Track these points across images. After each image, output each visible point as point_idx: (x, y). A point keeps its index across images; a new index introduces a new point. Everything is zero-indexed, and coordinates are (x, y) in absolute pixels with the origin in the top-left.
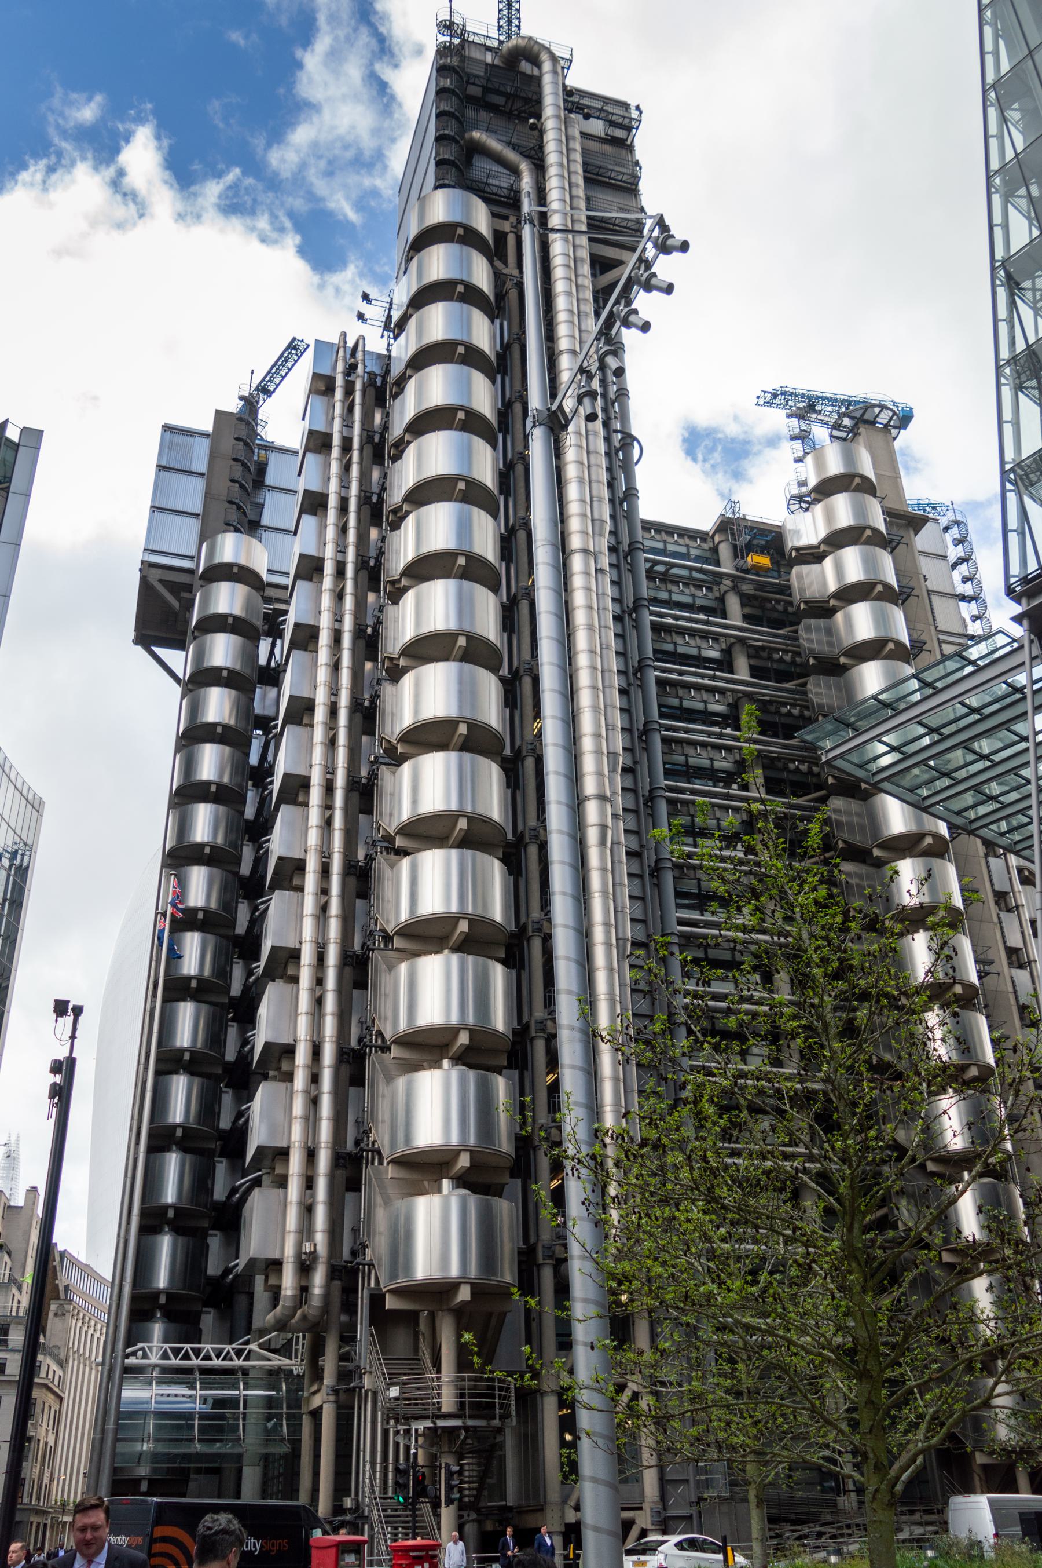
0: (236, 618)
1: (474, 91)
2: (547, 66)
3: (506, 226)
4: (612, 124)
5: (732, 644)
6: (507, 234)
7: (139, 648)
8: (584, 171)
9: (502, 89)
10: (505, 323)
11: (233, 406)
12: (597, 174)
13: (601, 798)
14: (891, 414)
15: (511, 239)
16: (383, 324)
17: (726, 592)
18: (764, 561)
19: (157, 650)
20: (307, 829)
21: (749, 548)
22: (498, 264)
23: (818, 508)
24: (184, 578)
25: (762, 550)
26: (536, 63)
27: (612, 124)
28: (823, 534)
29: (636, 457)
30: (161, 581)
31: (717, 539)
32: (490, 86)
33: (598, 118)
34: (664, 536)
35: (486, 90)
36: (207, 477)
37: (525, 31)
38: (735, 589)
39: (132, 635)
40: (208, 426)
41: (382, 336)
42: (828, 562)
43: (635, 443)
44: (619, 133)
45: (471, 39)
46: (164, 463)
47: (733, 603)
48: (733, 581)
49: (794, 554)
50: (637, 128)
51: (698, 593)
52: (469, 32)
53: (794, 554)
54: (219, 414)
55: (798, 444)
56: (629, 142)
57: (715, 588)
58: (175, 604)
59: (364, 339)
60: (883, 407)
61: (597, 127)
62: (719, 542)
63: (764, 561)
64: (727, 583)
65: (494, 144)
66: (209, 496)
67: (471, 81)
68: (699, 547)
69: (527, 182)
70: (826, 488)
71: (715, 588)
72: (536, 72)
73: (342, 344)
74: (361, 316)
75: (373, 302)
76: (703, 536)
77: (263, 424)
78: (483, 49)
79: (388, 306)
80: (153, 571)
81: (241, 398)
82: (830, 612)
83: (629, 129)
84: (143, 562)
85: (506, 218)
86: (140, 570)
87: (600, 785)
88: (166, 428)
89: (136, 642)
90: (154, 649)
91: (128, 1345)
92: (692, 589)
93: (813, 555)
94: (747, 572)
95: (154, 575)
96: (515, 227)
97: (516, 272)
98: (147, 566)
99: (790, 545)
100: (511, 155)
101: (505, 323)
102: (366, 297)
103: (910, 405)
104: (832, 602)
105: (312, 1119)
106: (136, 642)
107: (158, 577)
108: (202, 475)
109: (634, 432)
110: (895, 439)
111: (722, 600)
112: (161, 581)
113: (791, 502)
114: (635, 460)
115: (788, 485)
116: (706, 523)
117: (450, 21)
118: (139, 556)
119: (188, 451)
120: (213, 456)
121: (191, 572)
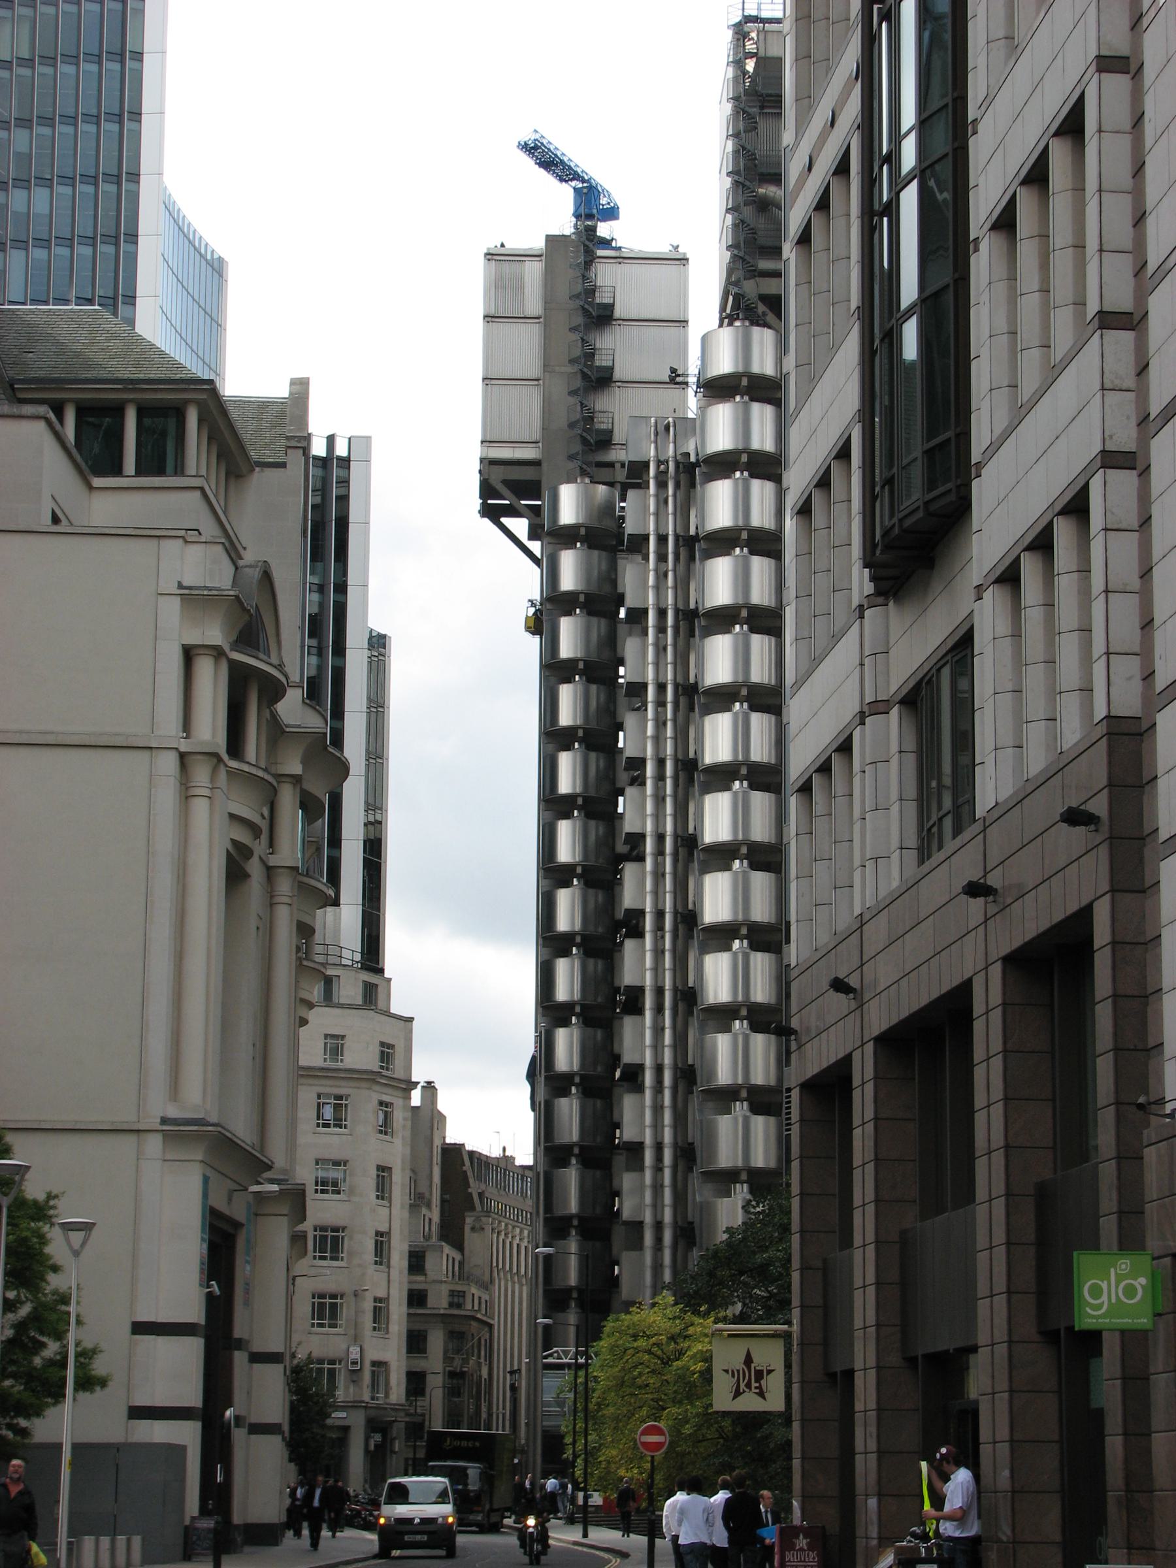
7: (486, 520)
19: (505, 520)
24: (527, 474)
36: (545, 320)
39: (477, 502)
40: (539, 244)
46: (492, 312)
66: (546, 366)
80: (495, 468)
84: (482, 460)
86: (480, 472)
88: (490, 256)
91: (546, 1348)
95: (497, 475)
98: (488, 464)
105: (657, 1205)
119: (517, 286)
120: (548, 300)
121: (536, 463)
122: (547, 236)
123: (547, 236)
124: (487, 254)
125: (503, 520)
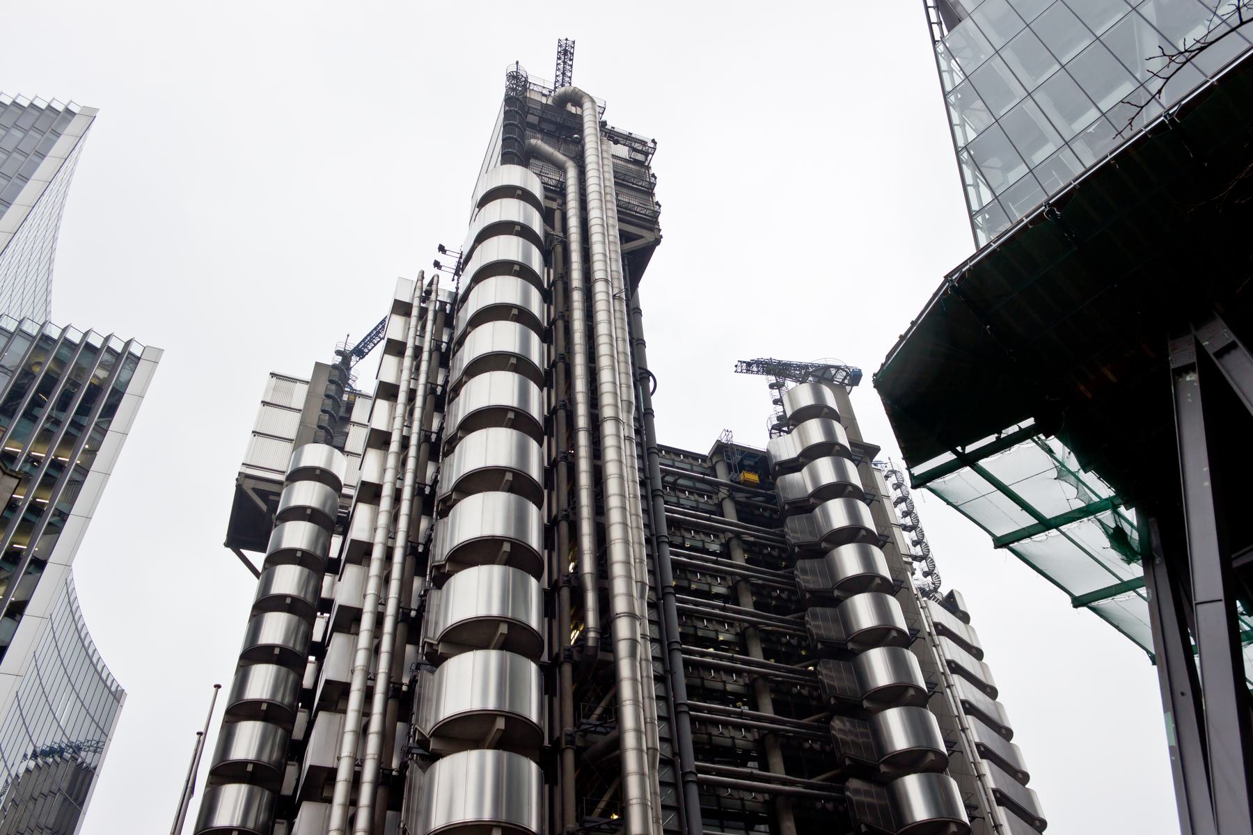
0: (313, 509)
1: (532, 119)
2: (587, 105)
3: (554, 205)
4: (635, 150)
5: (730, 539)
6: (554, 210)
7: (229, 550)
8: (615, 177)
9: (553, 119)
10: (552, 271)
11: (332, 359)
12: (623, 180)
13: (632, 615)
14: (844, 374)
15: (558, 215)
16: (454, 271)
17: (723, 499)
18: (753, 477)
19: (244, 552)
20: (356, 651)
21: (742, 467)
22: (549, 229)
23: (795, 432)
24: (274, 488)
25: (752, 469)
26: (578, 103)
27: (635, 150)
28: (799, 450)
29: (651, 390)
30: (254, 490)
31: (714, 460)
32: (544, 116)
33: (624, 145)
34: (673, 456)
35: (541, 119)
36: (304, 412)
37: (573, 85)
38: (730, 497)
39: (224, 538)
40: (308, 376)
41: (453, 280)
42: (805, 470)
43: (651, 378)
44: (640, 157)
45: (531, 88)
46: (268, 400)
47: (729, 508)
48: (728, 491)
49: (777, 468)
50: (653, 154)
51: (701, 500)
52: (530, 83)
53: (777, 468)
54: (319, 366)
55: (776, 393)
56: (646, 164)
57: (714, 496)
58: (264, 507)
59: (438, 277)
60: (838, 368)
61: (622, 151)
62: (717, 462)
63: (753, 477)
64: (724, 492)
65: (547, 148)
67: (531, 112)
68: (700, 466)
69: (572, 174)
70: (800, 416)
71: (714, 496)
72: (579, 112)
73: (420, 278)
74: (437, 264)
75: (447, 252)
76: (704, 458)
77: (354, 378)
78: (540, 95)
79: (459, 256)
81: (338, 353)
82: (810, 509)
83: (646, 154)
84: (240, 473)
85: (554, 200)
86: (237, 480)
87: (631, 604)
88: (273, 375)
89: (227, 544)
90: (243, 551)
92: (696, 496)
93: (794, 466)
94: (739, 483)
96: (561, 206)
97: (561, 235)
98: (243, 477)
99: (774, 461)
100: (560, 156)
101: (552, 271)
102: (442, 249)
103: (859, 367)
104: (812, 500)
106: (227, 544)
107: (252, 486)
108: (300, 410)
109: (649, 368)
110: (849, 393)
111: (720, 505)
112: (254, 490)
113: (773, 431)
114: (651, 390)
115: (770, 418)
116: (705, 449)
117: (517, 72)
118: (239, 468)
119: (290, 393)
120: (310, 395)
121: (280, 483)
122: (317, 364)
123: (317, 364)
124: (271, 374)
125: (243, 551)
